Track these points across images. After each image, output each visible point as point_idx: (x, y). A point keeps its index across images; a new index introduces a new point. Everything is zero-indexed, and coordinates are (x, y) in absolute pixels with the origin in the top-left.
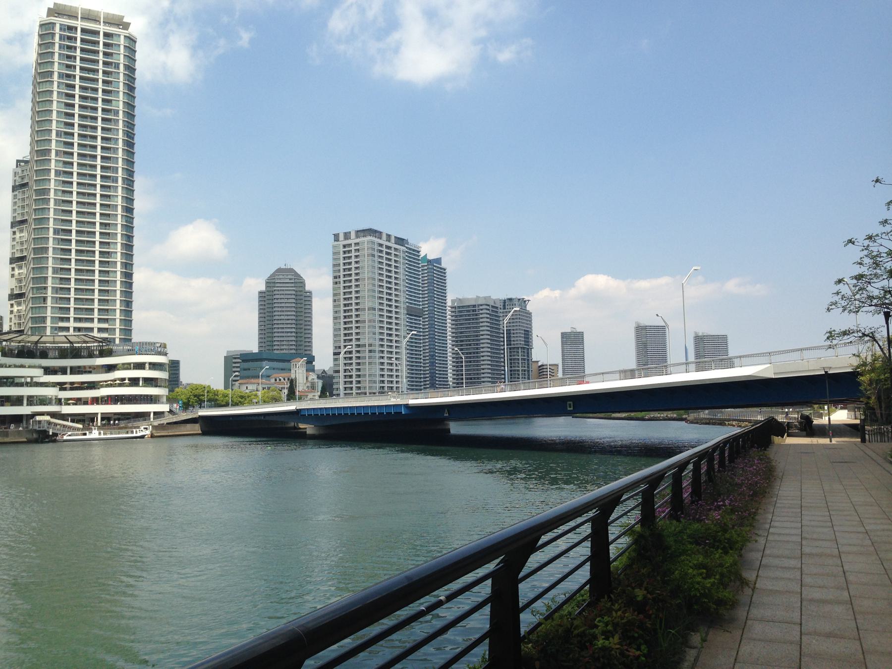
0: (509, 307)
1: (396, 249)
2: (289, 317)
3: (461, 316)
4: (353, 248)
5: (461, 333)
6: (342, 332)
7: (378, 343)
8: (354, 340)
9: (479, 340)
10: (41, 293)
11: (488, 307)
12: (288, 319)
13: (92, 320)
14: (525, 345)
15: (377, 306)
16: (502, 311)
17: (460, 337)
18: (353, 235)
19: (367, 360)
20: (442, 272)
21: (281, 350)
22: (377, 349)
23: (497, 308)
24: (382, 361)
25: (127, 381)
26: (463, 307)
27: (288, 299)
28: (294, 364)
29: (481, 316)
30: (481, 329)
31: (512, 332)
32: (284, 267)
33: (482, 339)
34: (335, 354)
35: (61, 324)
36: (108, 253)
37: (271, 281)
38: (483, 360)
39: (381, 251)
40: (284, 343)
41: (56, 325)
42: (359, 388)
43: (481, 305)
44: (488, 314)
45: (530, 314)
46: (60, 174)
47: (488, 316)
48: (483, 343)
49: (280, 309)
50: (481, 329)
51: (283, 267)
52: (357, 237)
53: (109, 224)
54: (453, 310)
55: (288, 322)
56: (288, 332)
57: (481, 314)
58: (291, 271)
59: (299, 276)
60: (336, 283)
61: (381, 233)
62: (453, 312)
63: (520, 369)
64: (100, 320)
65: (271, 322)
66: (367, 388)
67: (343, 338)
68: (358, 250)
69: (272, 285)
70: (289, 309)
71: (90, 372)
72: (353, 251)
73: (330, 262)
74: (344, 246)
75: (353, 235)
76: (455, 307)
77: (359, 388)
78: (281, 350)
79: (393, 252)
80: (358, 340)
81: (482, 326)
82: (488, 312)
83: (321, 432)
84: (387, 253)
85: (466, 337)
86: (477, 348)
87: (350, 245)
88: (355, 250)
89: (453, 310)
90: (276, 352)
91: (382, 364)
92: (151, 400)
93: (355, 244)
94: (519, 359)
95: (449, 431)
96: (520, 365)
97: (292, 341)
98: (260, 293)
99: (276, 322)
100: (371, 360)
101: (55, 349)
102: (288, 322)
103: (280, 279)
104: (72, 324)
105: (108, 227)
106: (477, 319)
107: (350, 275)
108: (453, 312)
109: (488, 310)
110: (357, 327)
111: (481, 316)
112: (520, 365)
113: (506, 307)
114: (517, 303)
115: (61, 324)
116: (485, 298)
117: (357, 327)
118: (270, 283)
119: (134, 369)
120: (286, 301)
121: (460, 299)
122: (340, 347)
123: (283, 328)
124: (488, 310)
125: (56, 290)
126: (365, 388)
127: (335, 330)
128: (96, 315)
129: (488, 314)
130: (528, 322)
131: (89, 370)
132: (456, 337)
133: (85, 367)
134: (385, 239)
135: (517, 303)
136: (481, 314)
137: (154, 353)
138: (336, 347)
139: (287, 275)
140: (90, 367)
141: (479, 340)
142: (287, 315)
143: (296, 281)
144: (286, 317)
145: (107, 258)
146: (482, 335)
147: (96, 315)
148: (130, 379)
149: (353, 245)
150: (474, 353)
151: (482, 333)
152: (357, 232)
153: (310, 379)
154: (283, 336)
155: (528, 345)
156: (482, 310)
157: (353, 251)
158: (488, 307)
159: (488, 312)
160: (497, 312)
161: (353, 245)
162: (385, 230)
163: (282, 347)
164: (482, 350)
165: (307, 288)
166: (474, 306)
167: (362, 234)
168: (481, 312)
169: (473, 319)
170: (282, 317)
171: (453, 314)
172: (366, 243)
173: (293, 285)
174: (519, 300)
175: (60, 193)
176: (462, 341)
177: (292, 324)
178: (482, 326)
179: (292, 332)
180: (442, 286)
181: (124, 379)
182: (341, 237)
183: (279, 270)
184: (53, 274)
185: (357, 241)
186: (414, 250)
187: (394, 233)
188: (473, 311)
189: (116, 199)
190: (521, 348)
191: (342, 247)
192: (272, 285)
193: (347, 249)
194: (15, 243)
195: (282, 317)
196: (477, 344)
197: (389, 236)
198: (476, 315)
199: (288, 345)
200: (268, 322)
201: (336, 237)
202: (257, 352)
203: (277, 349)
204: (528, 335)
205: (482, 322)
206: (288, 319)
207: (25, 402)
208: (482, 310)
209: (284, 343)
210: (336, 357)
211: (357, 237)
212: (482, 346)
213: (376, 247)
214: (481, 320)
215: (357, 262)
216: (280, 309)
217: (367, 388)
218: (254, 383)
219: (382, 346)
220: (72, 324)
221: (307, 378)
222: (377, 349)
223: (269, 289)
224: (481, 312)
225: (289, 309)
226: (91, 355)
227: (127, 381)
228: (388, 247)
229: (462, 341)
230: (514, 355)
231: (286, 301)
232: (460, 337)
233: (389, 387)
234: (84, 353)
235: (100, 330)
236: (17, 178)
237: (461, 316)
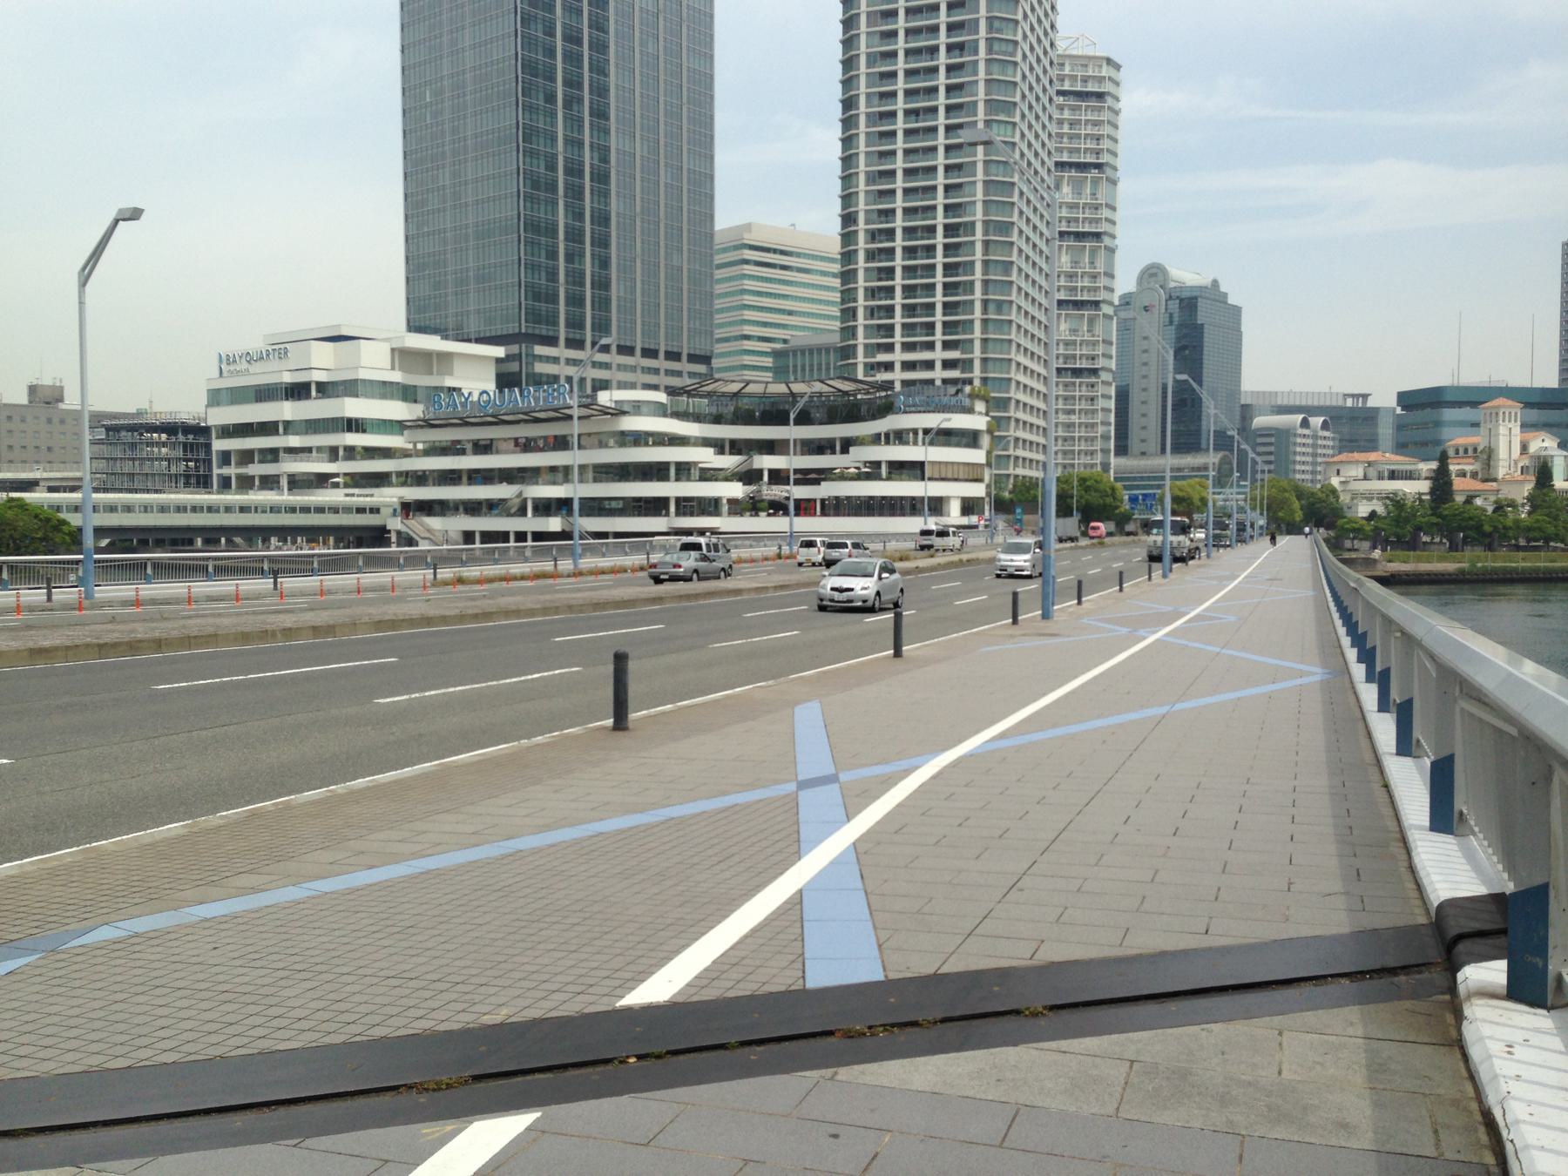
13: (930, 346)
28: (1494, 411)
35: (882, 357)
36: (959, 205)
41: (873, 360)
46: (875, 62)
64: (947, 345)
92: (860, 506)
104: (898, 356)
115: (882, 357)
137: (931, 409)
145: (959, 216)
147: (939, 336)
153: (1534, 447)
184: (866, 262)
202: (1556, 386)
207: (672, 508)
218: (1357, 462)
220: (898, 356)
221: (1524, 448)
235: (947, 364)
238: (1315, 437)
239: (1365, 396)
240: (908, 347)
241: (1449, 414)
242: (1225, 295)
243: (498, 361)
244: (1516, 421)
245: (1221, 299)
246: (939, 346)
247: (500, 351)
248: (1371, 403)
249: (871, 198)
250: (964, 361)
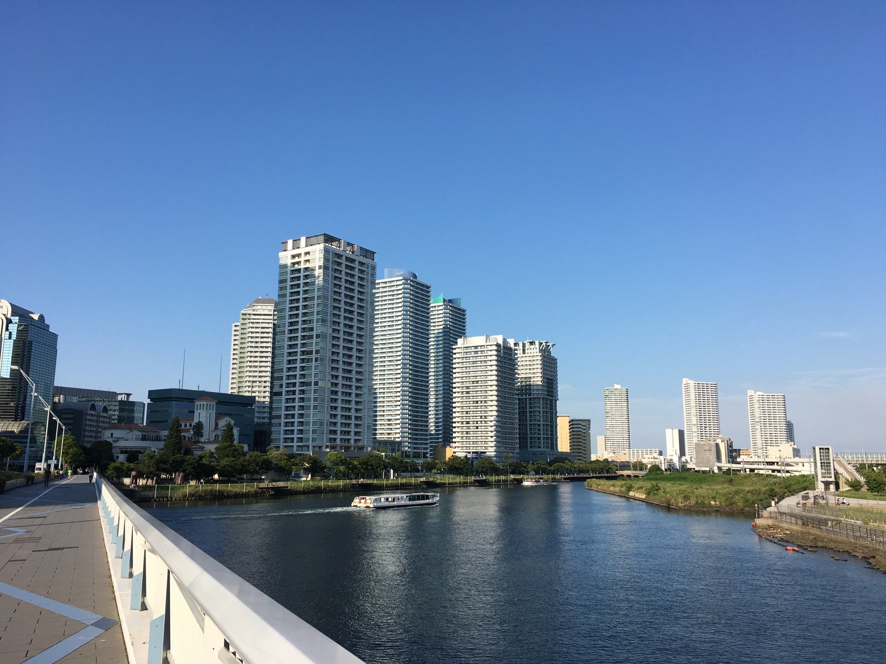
0: (529, 351)
1: (361, 264)
14: (548, 395)
16: (522, 355)
19: (312, 403)
20: (460, 314)
68: (308, 261)
73: (277, 279)
79: (356, 265)
80: (303, 376)
87: (299, 255)
113: (527, 351)
130: (553, 370)
149: (303, 255)
155: (552, 396)
161: (303, 255)
180: (460, 329)
186: (423, 285)
190: (543, 398)
191: (290, 257)
204: (552, 384)
221: (217, 424)
233: (345, 440)
238: (99, 416)
239: (128, 395)
242: (48, 326)
244: (213, 410)
245: (45, 328)
248: (131, 399)
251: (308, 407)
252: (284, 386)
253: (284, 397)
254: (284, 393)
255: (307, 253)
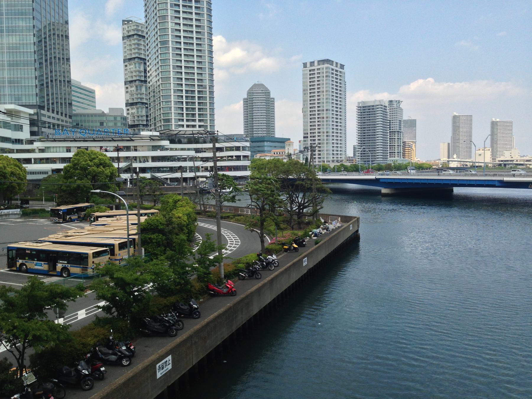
2: (262, 114)
3: (364, 112)
4: (316, 72)
5: (364, 123)
6: (309, 124)
7: (331, 131)
8: (316, 129)
9: (376, 127)
10: (168, 105)
11: (382, 107)
12: (262, 115)
13: (194, 120)
15: (331, 108)
17: (364, 125)
18: (316, 64)
21: (258, 134)
22: (331, 134)
23: (386, 107)
24: (333, 141)
25: (234, 158)
26: (365, 107)
27: (261, 103)
29: (377, 112)
30: (377, 120)
31: (391, 122)
32: (257, 83)
33: (377, 127)
34: (304, 137)
36: (202, 80)
37: (251, 92)
38: (378, 140)
39: (333, 73)
40: (260, 130)
42: (320, 158)
43: (378, 105)
44: (381, 111)
45: (402, 110)
47: (382, 112)
48: (378, 129)
49: (257, 109)
50: (377, 120)
51: (257, 83)
52: (319, 64)
53: (201, 62)
54: (360, 108)
55: (262, 117)
56: (261, 123)
57: (378, 111)
58: (262, 85)
59: (267, 88)
60: (305, 94)
61: (333, 61)
62: (359, 110)
63: (396, 144)
64: (200, 121)
65: (251, 117)
66: (325, 158)
67: (309, 128)
68: (319, 73)
69: (251, 94)
70: (262, 109)
71: (205, 152)
72: (316, 74)
74: (310, 71)
75: (316, 64)
76: (361, 107)
77: (320, 158)
78: (258, 134)
81: (378, 119)
82: (382, 109)
83: (393, 192)
84: (336, 75)
85: (368, 125)
86: (374, 132)
87: (314, 70)
88: (317, 73)
89: (360, 108)
90: (255, 135)
91: (333, 143)
93: (317, 69)
94: (395, 139)
95: (452, 191)
96: (396, 142)
97: (264, 128)
98: (244, 99)
99: (254, 117)
100: (327, 142)
101: (186, 137)
102: (262, 117)
103: (256, 90)
104: (185, 123)
105: (200, 64)
106: (374, 114)
107: (314, 89)
108: (359, 110)
109: (382, 108)
110: (318, 121)
111: (377, 112)
112: (396, 142)
114: (395, 103)
116: (380, 101)
117: (318, 121)
118: (250, 93)
119: (236, 150)
120: (260, 104)
121: (363, 102)
122: (307, 134)
123: (259, 121)
124: (382, 108)
125: (176, 103)
126: (324, 158)
127: (304, 122)
128: (197, 118)
129: (381, 111)
131: (204, 150)
132: (361, 126)
133: (202, 148)
134: (339, 67)
135: (395, 103)
136: (378, 111)
138: (305, 134)
139: (260, 88)
140: (205, 149)
141: (376, 127)
142: (261, 113)
143: (266, 91)
144: (260, 114)
146: (378, 124)
147: (197, 118)
148: (236, 156)
149: (316, 70)
150: (372, 135)
151: (377, 123)
152: (319, 61)
154: (259, 126)
155: (401, 130)
156: (378, 108)
157: (316, 74)
158: (382, 107)
159: (382, 109)
160: (386, 109)
161: (316, 70)
162: (335, 60)
163: (259, 132)
164: (377, 133)
165: (272, 96)
166: (373, 106)
167: (322, 63)
168: (377, 110)
169: (372, 114)
170: (258, 114)
171: (359, 111)
172: (325, 69)
173: (264, 94)
174: (396, 101)
175: (174, 43)
176: (364, 128)
177: (264, 118)
178: (378, 119)
179: (264, 123)
181: (232, 157)
182: (308, 65)
183: (255, 85)
185: (319, 67)
187: (340, 62)
188: (372, 109)
189: (204, 46)
191: (308, 71)
192: (251, 94)
193: (312, 72)
194: (127, 72)
195: (258, 114)
196: (374, 130)
197: (337, 63)
198: (374, 112)
199: (262, 131)
200: (250, 117)
201: (305, 65)
203: (256, 134)
205: (378, 116)
206: (262, 115)
208: (378, 108)
209: (260, 130)
210: (305, 139)
211: (319, 64)
212: (377, 131)
213: (331, 71)
214: (377, 115)
215: (318, 81)
216: (257, 109)
217: (325, 158)
219: (333, 132)
220: (185, 123)
222: (331, 134)
223: (250, 97)
224: (377, 110)
225: (262, 109)
226: (205, 142)
227: (234, 158)
228: (337, 71)
229: (364, 128)
230: (392, 136)
231: (260, 104)
232: (364, 125)
234: (201, 140)
235: (200, 126)
236: (125, 32)
237: (364, 112)
240: (188, 120)
241: (266, 144)
243: (30, 115)
246: (197, 121)
247: (31, 111)
249: (174, 73)
250: (205, 126)
251: (323, 143)
252: (309, 133)
253: (309, 138)
254: (309, 137)
255: (318, 69)
